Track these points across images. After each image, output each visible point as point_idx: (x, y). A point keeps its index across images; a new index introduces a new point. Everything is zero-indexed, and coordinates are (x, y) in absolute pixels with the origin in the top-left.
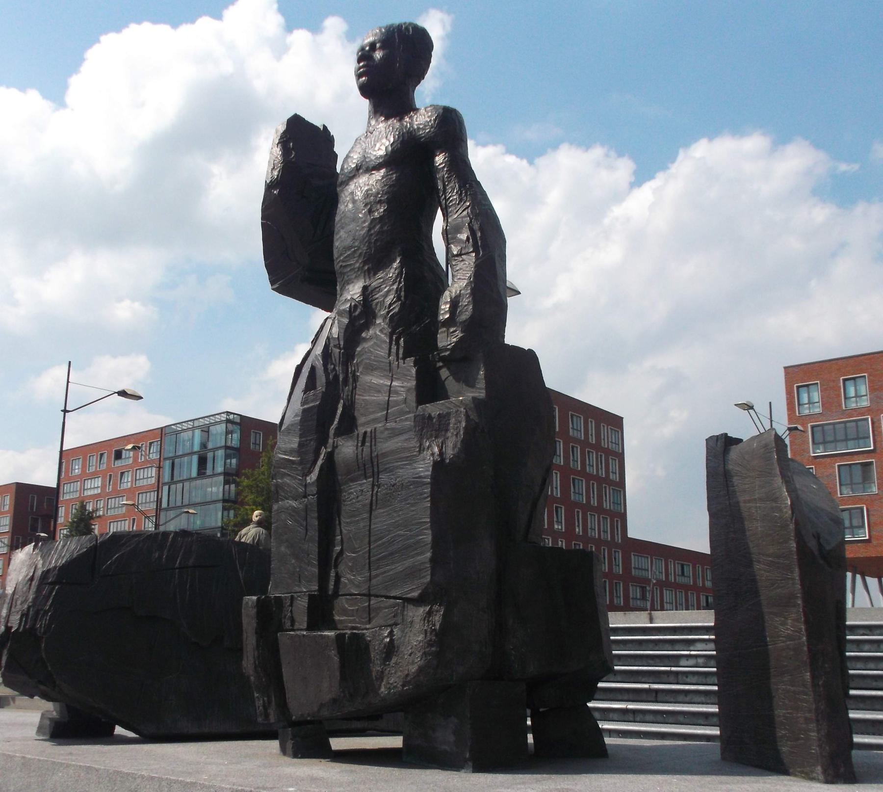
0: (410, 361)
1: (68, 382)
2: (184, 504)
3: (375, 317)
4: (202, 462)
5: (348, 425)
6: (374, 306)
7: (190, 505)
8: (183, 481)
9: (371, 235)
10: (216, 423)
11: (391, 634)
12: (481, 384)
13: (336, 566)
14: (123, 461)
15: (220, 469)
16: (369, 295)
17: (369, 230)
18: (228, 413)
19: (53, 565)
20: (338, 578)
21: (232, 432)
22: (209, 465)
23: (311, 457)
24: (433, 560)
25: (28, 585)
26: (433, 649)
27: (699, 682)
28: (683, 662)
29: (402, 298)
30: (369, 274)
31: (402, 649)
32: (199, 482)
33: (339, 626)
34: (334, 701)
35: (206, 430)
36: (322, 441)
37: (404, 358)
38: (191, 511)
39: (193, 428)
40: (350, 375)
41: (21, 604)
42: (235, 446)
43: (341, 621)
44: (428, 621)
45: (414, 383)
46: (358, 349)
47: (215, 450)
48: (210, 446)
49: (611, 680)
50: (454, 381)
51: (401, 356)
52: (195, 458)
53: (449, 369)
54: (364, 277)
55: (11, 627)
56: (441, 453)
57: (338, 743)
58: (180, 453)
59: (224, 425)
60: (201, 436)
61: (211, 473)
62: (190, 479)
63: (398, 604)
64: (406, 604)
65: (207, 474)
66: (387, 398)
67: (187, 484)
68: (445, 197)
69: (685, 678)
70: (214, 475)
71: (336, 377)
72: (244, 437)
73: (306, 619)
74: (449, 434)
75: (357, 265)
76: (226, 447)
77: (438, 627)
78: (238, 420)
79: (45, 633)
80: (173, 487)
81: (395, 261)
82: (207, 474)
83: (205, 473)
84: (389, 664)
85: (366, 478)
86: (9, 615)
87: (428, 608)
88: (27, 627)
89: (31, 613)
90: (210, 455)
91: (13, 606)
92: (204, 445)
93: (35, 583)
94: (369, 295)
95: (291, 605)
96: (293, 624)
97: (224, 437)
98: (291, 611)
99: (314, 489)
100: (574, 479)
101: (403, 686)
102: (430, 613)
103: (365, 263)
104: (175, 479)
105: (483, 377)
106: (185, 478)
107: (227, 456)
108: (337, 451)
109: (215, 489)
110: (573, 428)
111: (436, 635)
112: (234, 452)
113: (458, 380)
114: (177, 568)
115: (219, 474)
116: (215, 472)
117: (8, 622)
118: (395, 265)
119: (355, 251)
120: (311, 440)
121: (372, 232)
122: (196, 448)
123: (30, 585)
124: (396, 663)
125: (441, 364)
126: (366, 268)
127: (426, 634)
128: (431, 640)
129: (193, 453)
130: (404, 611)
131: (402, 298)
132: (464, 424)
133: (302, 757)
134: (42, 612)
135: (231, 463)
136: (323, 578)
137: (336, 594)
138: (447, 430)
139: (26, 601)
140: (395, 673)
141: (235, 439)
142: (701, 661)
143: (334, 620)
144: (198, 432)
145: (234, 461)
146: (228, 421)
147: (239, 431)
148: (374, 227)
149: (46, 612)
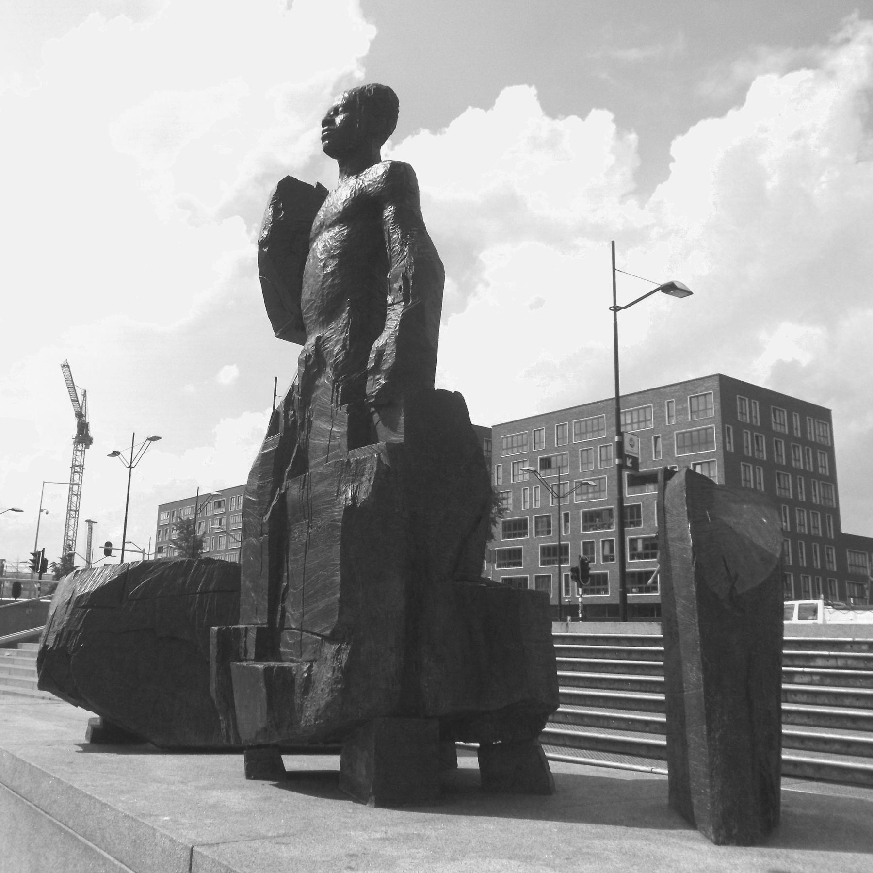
0: (345, 407)
1: (275, 396)
3: (325, 366)
5: (302, 465)
6: (325, 356)
9: (324, 288)
11: (310, 669)
12: (401, 428)
13: (283, 602)
16: (321, 345)
17: (323, 284)
19: (87, 591)
20: (284, 610)
23: (268, 498)
24: (341, 600)
25: (65, 609)
26: (339, 686)
28: (797, 679)
30: (323, 325)
31: (317, 684)
33: (283, 658)
34: (265, 729)
36: (278, 483)
37: (341, 405)
40: (306, 420)
41: (58, 625)
43: (284, 653)
44: (337, 659)
45: (346, 429)
46: (313, 396)
50: (383, 426)
51: (339, 403)
53: (379, 414)
54: (320, 327)
55: (48, 646)
56: (354, 498)
57: (292, 763)
63: (317, 641)
64: (324, 641)
66: (328, 443)
68: (390, 248)
69: (793, 696)
71: (295, 422)
73: (254, 650)
74: (364, 479)
75: (314, 317)
77: (343, 665)
79: (74, 652)
81: (343, 311)
84: (307, 698)
85: (305, 518)
86: (48, 635)
88: (60, 645)
89: (65, 634)
91: (52, 626)
93: (71, 606)
94: (321, 345)
95: (246, 636)
96: (246, 655)
98: (245, 642)
99: (266, 529)
100: (779, 474)
101: (316, 720)
102: (339, 651)
103: (320, 315)
105: (403, 422)
108: (288, 492)
110: (776, 423)
111: (342, 673)
113: (385, 424)
114: (198, 593)
117: (46, 641)
118: (345, 315)
119: (312, 305)
123: (67, 607)
124: (312, 698)
125: (373, 409)
126: (321, 319)
127: (334, 672)
128: (337, 678)
130: (321, 648)
131: (348, 347)
132: (375, 469)
133: (254, 779)
134: (74, 633)
136: (272, 611)
137: (282, 628)
138: (363, 475)
139: (61, 622)
140: (311, 707)
142: (816, 678)
143: (280, 652)
148: (327, 280)
149: (77, 633)
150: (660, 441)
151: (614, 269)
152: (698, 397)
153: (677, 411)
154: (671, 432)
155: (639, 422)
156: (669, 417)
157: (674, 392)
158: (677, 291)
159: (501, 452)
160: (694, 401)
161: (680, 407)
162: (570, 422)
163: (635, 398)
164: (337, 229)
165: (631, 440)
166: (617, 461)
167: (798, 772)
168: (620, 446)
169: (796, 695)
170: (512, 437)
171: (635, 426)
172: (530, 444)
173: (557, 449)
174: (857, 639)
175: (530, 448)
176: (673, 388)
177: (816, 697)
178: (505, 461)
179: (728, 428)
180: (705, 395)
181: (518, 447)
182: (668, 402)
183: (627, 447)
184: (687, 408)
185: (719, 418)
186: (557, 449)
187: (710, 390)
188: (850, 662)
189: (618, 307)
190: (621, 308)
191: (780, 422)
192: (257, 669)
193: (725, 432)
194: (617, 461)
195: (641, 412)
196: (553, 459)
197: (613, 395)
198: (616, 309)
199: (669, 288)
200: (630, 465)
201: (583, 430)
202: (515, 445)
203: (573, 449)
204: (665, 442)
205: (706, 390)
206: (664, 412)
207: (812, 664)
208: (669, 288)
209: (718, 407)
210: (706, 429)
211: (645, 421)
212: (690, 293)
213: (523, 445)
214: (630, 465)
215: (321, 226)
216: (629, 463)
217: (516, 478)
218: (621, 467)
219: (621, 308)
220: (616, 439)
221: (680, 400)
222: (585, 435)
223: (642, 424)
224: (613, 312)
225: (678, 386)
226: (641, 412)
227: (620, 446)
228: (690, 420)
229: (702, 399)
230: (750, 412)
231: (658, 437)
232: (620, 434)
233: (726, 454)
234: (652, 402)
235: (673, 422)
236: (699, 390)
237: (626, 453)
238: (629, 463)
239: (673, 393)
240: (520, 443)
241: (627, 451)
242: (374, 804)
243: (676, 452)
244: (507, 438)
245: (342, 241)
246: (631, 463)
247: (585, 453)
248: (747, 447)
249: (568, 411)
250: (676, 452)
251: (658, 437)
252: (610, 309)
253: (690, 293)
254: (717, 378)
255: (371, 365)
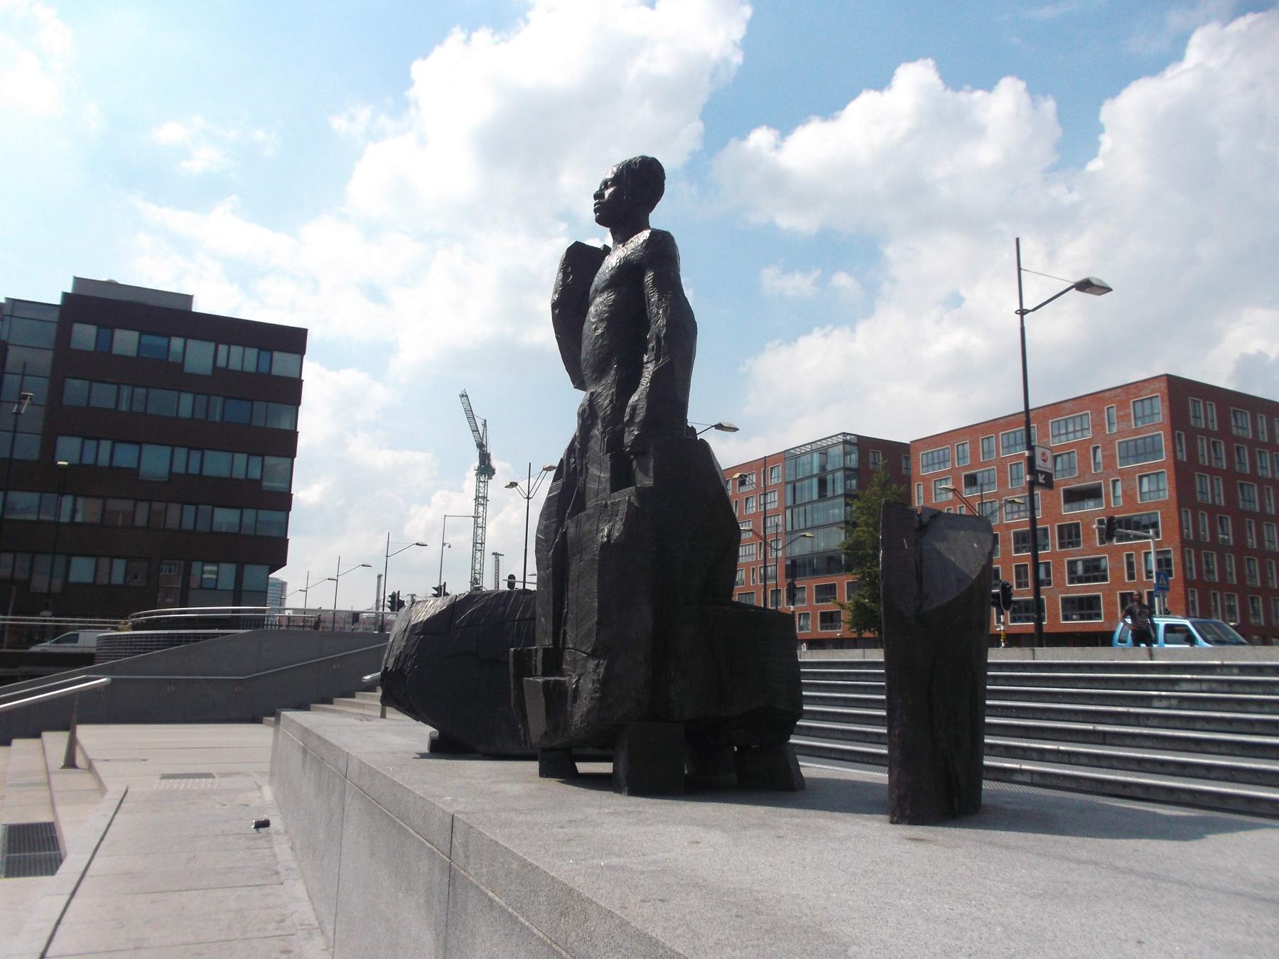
2: (807, 527)
4: (822, 484)
5: (580, 505)
7: (806, 529)
8: (805, 504)
9: (595, 349)
10: (834, 445)
12: (651, 474)
13: (565, 625)
14: (747, 487)
15: (840, 491)
17: (594, 345)
18: (844, 433)
20: (565, 633)
21: (850, 453)
22: (830, 487)
24: (598, 623)
26: (597, 695)
27: (1161, 725)
29: (614, 402)
32: (821, 504)
33: (565, 674)
35: (824, 452)
36: (561, 523)
37: (607, 453)
38: (808, 534)
39: (812, 451)
40: (584, 467)
42: (854, 467)
43: (565, 669)
45: (609, 475)
47: (833, 472)
48: (829, 468)
49: (1073, 719)
52: (815, 481)
56: (609, 535)
58: (800, 476)
59: (841, 447)
60: (820, 459)
61: (832, 495)
62: (811, 502)
65: (828, 496)
67: (809, 507)
70: (835, 497)
72: (863, 457)
75: (589, 375)
76: (845, 469)
77: (601, 677)
78: (855, 441)
80: (796, 510)
81: (611, 369)
82: (828, 496)
83: (826, 496)
87: (596, 662)
90: (829, 477)
92: (823, 468)
95: (536, 656)
96: (536, 672)
97: (842, 458)
101: (581, 724)
102: (597, 666)
103: (593, 372)
104: (797, 502)
106: (807, 501)
107: (847, 478)
109: (836, 511)
111: (600, 684)
112: (851, 473)
113: (640, 470)
115: (840, 496)
116: (836, 494)
118: (613, 372)
120: (553, 522)
121: (596, 347)
122: (816, 471)
125: (632, 457)
126: (594, 377)
127: (593, 683)
129: (811, 476)
131: (614, 402)
135: (851, 484)
137: (564, 648)
138: (617, 515)
141: (853, 460)
144: (816, 456)
145: (854, 482)
146: (845, 442)
147: (857, 451)
150: (1099, 452)
151: (1019, 269)
152: (1142, 400)
153: (1119, 417)
154: (1112, 442)
155: (1075, 431)
156: (1109, 424)
157: (1116, 396)
158: (1094, 288)
159: (922, 468)
160: (1138, 405)
161: (1122, 413)
162: (997, 434)
163: (1070, 405)
164: (605, 296)
165: (1044, 454)
166: (1028, 478)
167: (1127, 792)
168: (1031, 461)
169: (1148, 719)
170: (932, 452)
171: (1071, 436)
172: (953, 459)
173: (983, 465)
174: (1226, 662)
175: (953, 464)
176: (1112, 392)
177: (1167, 720)
178: (924, 479)
179: (1179, 435)
180: (1151, 398)
181: (939, 463)
182: (1108, 408)
183: (1038, 461)
184: (1129, 414)
185: (1167, 422)
186: (983, 465)
187: (1156, 392)
188: (1214, 685)
189: (1026, 310)
190: (1028, 311)
191: (1242, 425)
192: (538, 682)
193: (1174, 440)
194: (1028, 478)
195: (1078, 421)
196: (979, 476)
197: (1022, 409)
198: (1022, 312)
199: (1085, 286)
200: (1043, 482)
201: (1012, 443)
202: (936, 461)
203: (1001, 464)
204: (1106, 453)
205: (1152, 393)
206: (1103, 419)
207: (1177, 688)
208: (1085, 286)
209: (1166, 411)
210: (1152, 437)
211: (1082, 430)
212: (1109, 290)
213: (944, 462)
214: (1043, 482)
215: (596, 291)
216: (1041, 479)
217: (938, 497)
218: (1032, 485)
219: (1028, 311)
220: (1027, 453)
221: (1122, 405)
222: (1014, 449)
223: (1079, 434)
224: (1019, 316)
225: (1120, 390)
226: (1078, 421)
227: (1031, 461)
228: (1133, 427)
229: (1147, 403)
230: (1205, 416)
231: (1098, 447)
232: (1030, 448)
233: (1178, 465)
234: (1088, 409)
235: (1115, 429)
236: (1143, 392)
237: (1038, 468)
238: (1041, 479)
239: (1113, 397)
240: (941, 460)
241: (1039, 466)
242: (626, 793)
243: (1118, 463)
244: (927, 454)
245: (609, 306)
246: (1044, 479)
247: (1014, 467)
248: (1203, 455)
249: (992, 423)
250: (1118, 463)
251: (1098, 447)
252: (1016, 312)
253: (1109, 290)
254: (1165, 378)
255: (626, 418)
